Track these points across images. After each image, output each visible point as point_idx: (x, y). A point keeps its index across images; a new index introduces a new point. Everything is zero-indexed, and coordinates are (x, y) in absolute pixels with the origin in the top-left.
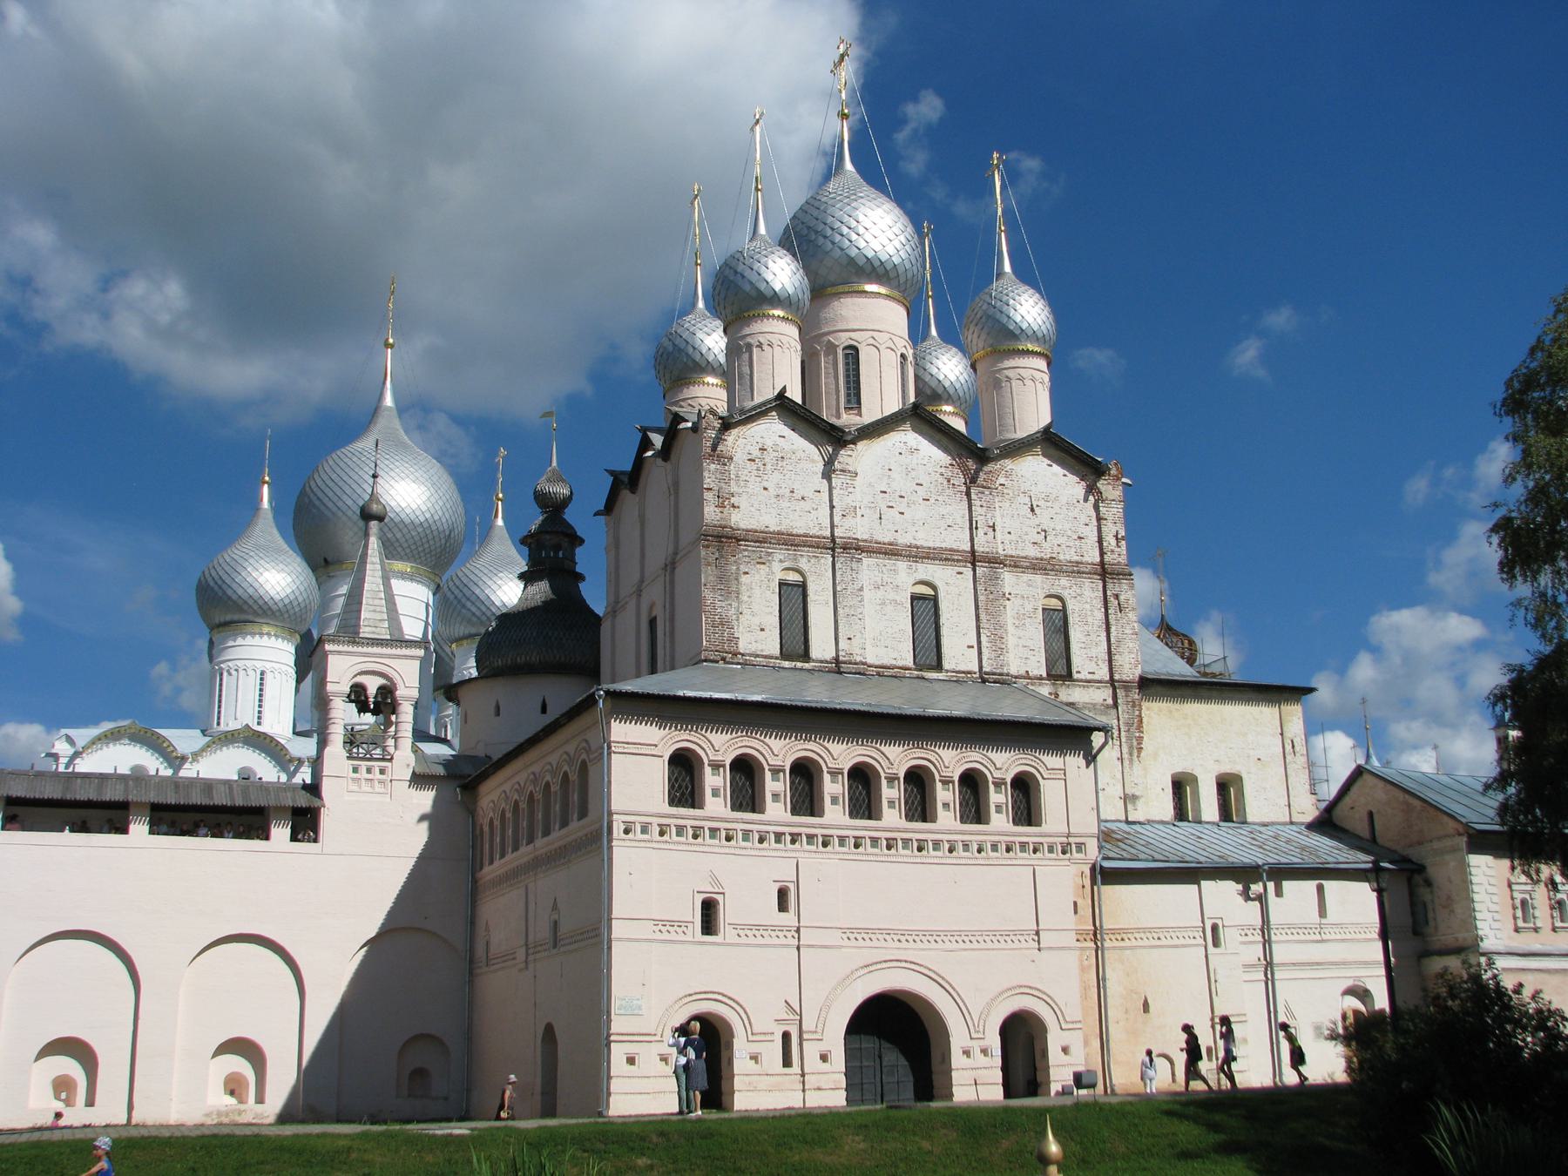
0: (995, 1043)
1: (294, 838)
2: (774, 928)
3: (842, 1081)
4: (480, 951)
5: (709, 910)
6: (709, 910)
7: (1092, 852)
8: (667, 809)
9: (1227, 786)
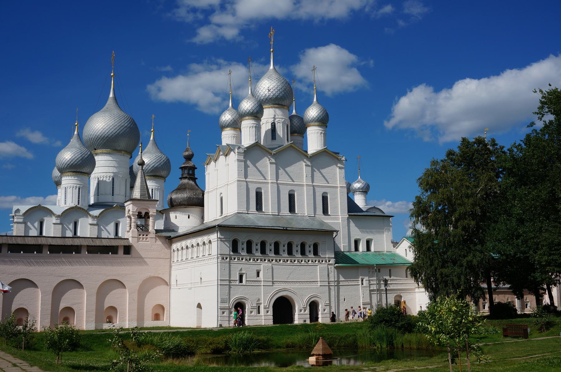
0: (308, 307)
1: (124, 254)
2: (256, 281)
3: (272, 317)
4: (173, 282)
5: (241, 277)
6: (241, 277)
7: (332, 261)
8: (232, 253)
9: (368, 243)
